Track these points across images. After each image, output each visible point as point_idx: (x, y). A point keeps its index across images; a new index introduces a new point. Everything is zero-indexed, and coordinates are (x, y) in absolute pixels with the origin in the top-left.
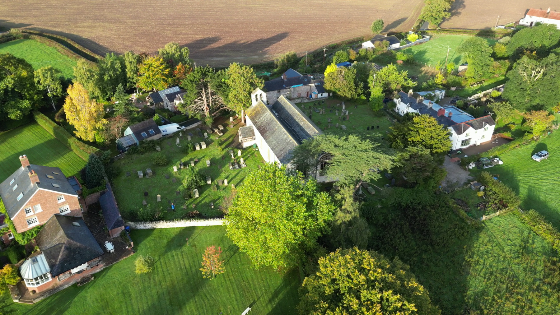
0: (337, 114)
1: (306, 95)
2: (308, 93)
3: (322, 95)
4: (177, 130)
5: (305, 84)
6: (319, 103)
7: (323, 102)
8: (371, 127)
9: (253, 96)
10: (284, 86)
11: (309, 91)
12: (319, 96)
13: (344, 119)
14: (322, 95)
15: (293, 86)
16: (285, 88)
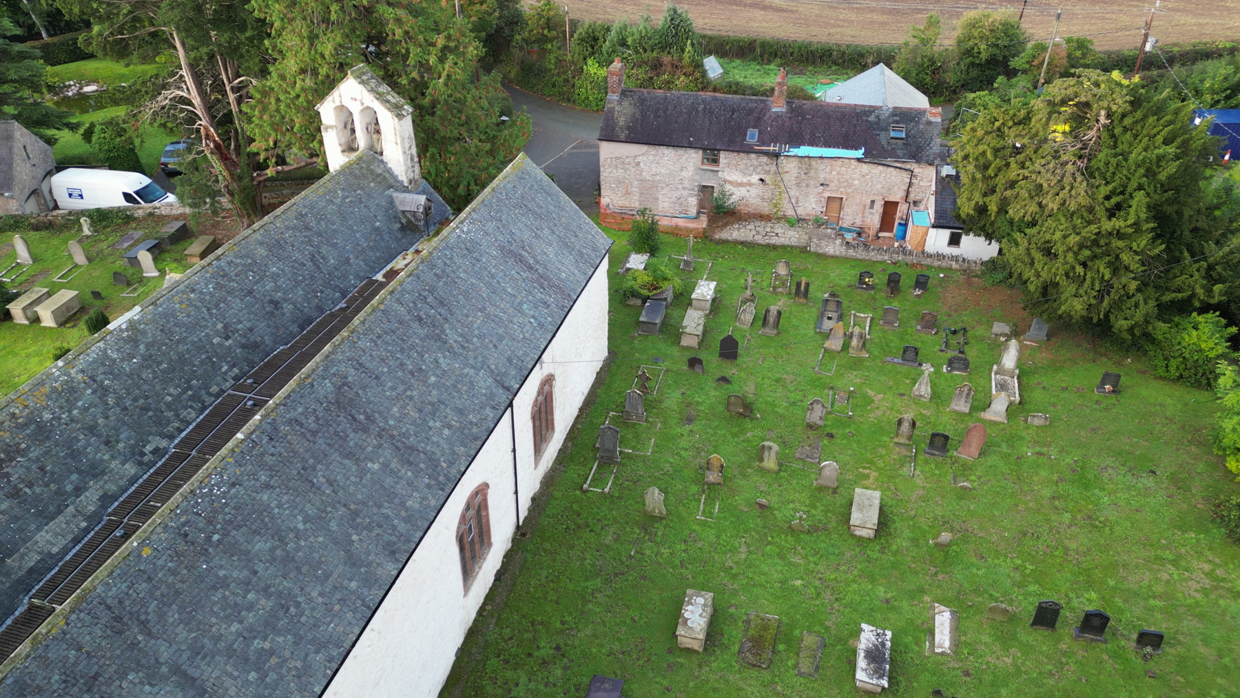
0: (923, 389)
1: (873, 220)
2: (890, 207)
3: (954, 241)
4: (123, 203)
5: (876, 154)
6: (894, 283)
7: (922, 283)
8: (1070, 618)
9: (327, 111)
10: (752, 136)
11: (897, 196)
12: (938, 240)
13: (939, 442)
14: (954, 241)
15: (804, 150)
16: (749, 150)
